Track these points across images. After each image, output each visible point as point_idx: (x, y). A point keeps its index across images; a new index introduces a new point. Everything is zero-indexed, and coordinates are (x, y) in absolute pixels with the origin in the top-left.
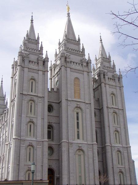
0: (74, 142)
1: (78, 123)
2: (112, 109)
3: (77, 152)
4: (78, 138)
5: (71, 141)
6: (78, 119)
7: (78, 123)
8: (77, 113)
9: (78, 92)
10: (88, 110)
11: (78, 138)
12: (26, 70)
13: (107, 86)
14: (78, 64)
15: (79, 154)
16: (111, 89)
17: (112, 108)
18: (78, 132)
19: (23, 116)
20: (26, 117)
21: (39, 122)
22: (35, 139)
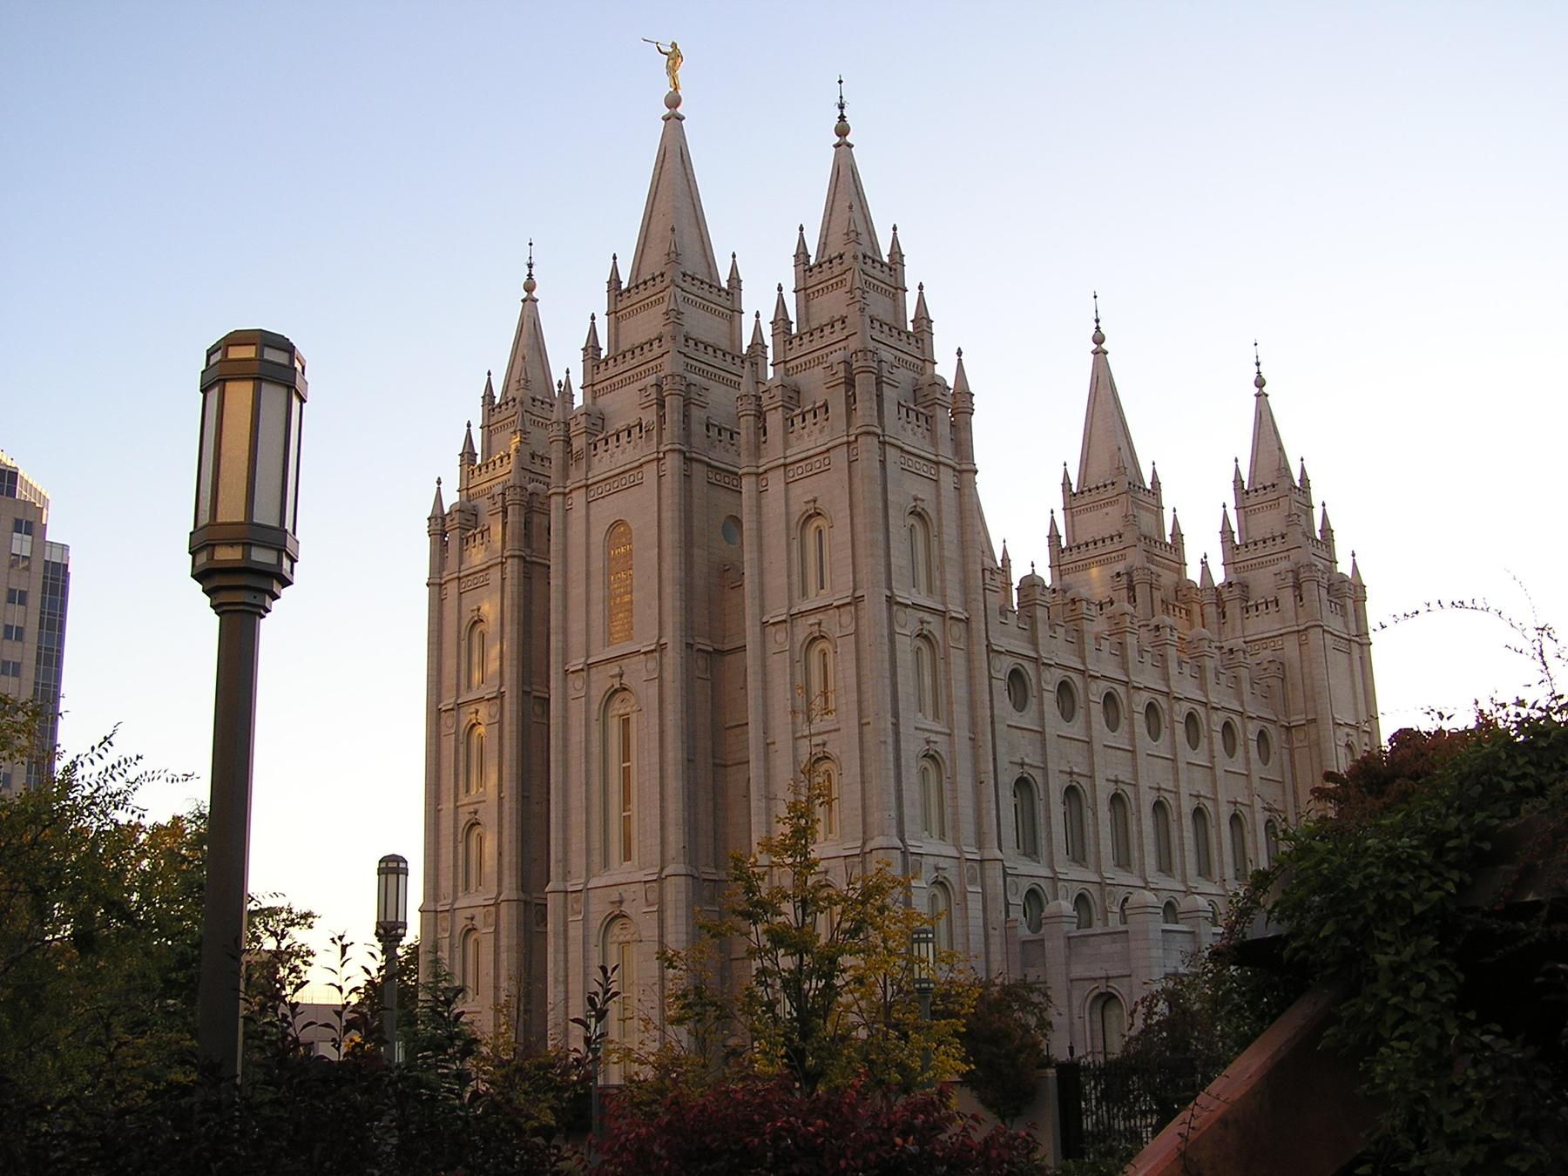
0: (593, 883)
1: (626, 773)
2: (800, 621)
3: (616, 929)
4: (627, 856)
5: (575, 884)
6: (626, 756)
7: (626, 773)
8: (626, 722)
9: (627, 598)
10: (654, 690)
11: (627, 856)
12: (452, 590)
13: (775, 482)
14: (624, 437)
15: (621, 938)
16: (797, 490)
17: (802, 614)
18: (627, 820)
19: (447, 806)
20: (456, 807)
21: (489, 816)
22: (480, 901)
